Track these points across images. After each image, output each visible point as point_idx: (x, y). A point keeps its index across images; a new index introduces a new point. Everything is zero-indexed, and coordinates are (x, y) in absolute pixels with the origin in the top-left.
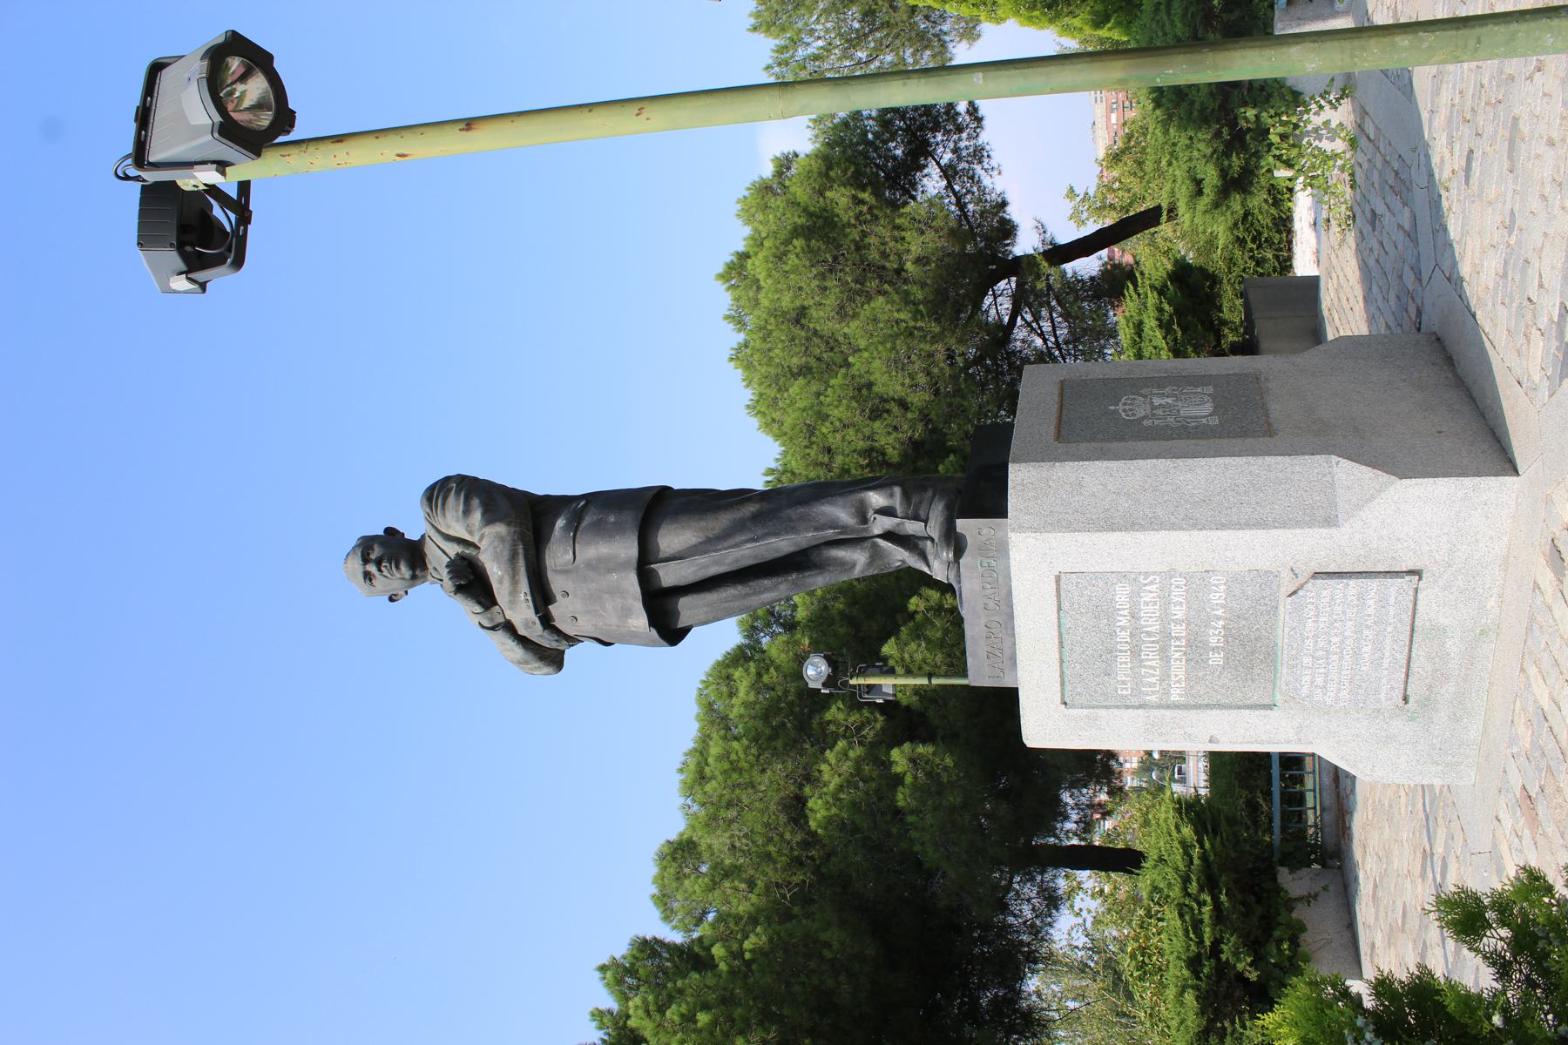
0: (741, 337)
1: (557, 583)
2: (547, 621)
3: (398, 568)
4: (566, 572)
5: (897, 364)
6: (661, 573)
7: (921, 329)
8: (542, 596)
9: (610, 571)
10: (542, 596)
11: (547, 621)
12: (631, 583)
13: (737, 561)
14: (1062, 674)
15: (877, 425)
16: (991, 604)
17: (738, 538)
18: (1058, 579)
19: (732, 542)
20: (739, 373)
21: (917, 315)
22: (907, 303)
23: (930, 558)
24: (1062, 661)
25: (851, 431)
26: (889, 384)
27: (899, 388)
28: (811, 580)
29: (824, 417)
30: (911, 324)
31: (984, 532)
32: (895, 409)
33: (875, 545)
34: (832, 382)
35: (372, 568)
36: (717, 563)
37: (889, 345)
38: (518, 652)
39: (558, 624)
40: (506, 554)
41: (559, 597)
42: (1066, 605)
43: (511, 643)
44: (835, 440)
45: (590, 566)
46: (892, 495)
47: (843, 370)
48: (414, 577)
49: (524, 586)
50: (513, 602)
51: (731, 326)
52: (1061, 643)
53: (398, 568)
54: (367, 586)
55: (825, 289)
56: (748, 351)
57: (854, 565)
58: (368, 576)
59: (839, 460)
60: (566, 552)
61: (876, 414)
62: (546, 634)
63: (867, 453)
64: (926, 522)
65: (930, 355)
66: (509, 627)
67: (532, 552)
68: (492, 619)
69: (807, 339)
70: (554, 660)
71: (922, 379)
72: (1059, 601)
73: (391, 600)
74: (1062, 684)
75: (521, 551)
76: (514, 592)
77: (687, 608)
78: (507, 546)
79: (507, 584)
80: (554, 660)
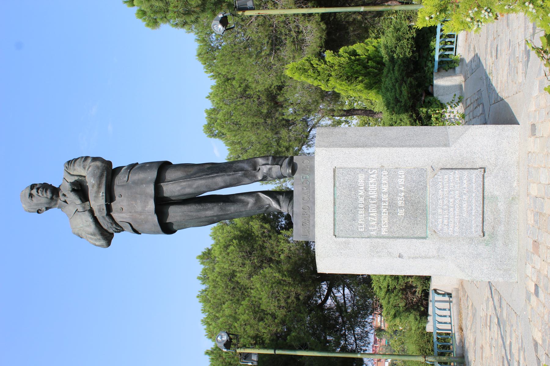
0: (203, 287)
1: (117, 191)
2: (109, 209)
3: (46, 192)
4: (123, 186)
5: (274, 296)
6: (165, 188)
7: (284, 281)
8: (110, 197)
9: (142, 184)
10: (110, 197)
11: (109, 209)
12: (151, 190)
13: (198, 187)
14: (334, 219)
15: (261, 323)
16: (306, 198)
17: (200, 174)
18: (334, 171)
19: (197, 175)
20: (200, 306)
21: (284, 275)
22: (279, 272)
23: (281, 203)
24: (334, 213)
25: (248, 327)
26: (269, 305)
27: (272, 308)
28: (228, 208)
29: (236, 319)
30: (281, 278)
31: (305, 162)
32: (269, 317)
33: (258, 196)
34: (243, 303)
35: (34, 192)
36: (190, 186)
37: (270, 286)
38: (92, 228)
39: (113, 214)
40: (99, 174)
41: (117, 198)
42: (337, 184)
43: (90, 220)
44: (240, 331)
45: (135, 183)
46: (268, 159)
47: (247, 299)
48: (52, 198)
49: (103, 190)
50: (96, 197)
51: (200, 281)
52: (334, 203)
53: (46, 192)
54: (29, 200)
55: (244, 264)
56: (207, 292)
57: (248, 203)
58: (31, 195)
59: (242, 340)
60: (125, 177)
61: (261, 319)
62: (107, 218)
63: (256, 337)
64: (281, 166)
65: (288, 293)
66: (91, 211)
67: (110, 177)
68: (84, 208)
69: (234, 288)
70: (107, 237)
71: (283, 304)
72: (334, 182)
73: (38, 212)
74: (334, 225)
75: (105, 174)
76: (98, 192)
77: (174, 214)
78: (100, 171)
79: (95, 188)
80: (107, 237)
